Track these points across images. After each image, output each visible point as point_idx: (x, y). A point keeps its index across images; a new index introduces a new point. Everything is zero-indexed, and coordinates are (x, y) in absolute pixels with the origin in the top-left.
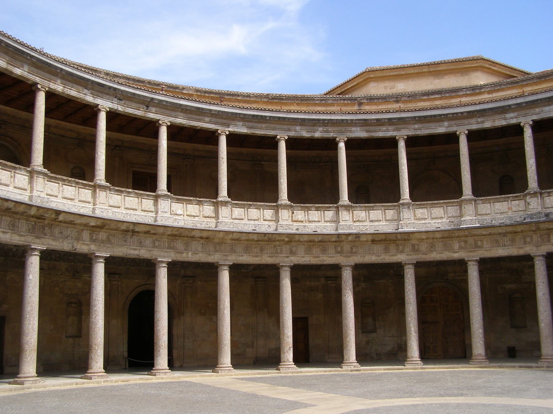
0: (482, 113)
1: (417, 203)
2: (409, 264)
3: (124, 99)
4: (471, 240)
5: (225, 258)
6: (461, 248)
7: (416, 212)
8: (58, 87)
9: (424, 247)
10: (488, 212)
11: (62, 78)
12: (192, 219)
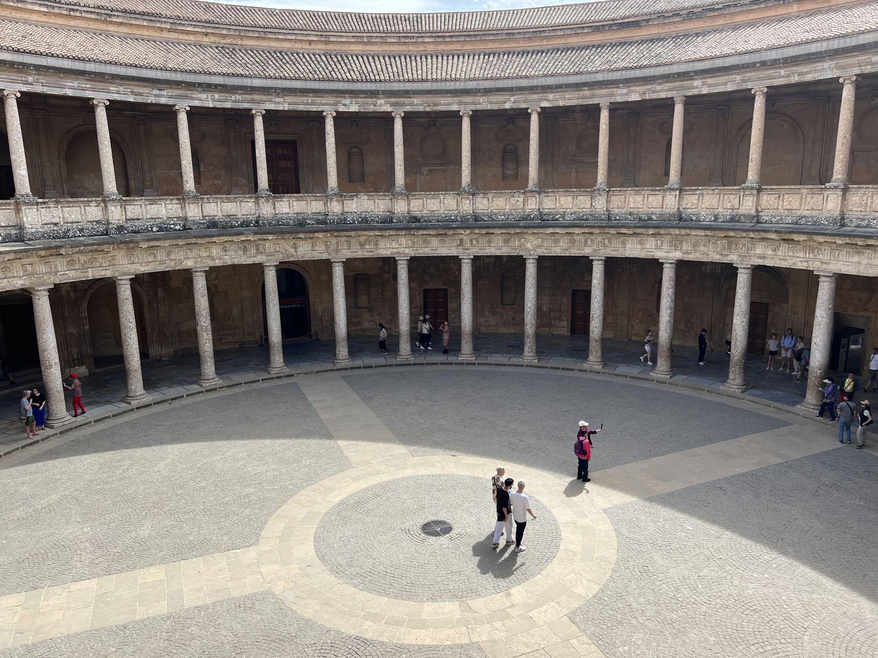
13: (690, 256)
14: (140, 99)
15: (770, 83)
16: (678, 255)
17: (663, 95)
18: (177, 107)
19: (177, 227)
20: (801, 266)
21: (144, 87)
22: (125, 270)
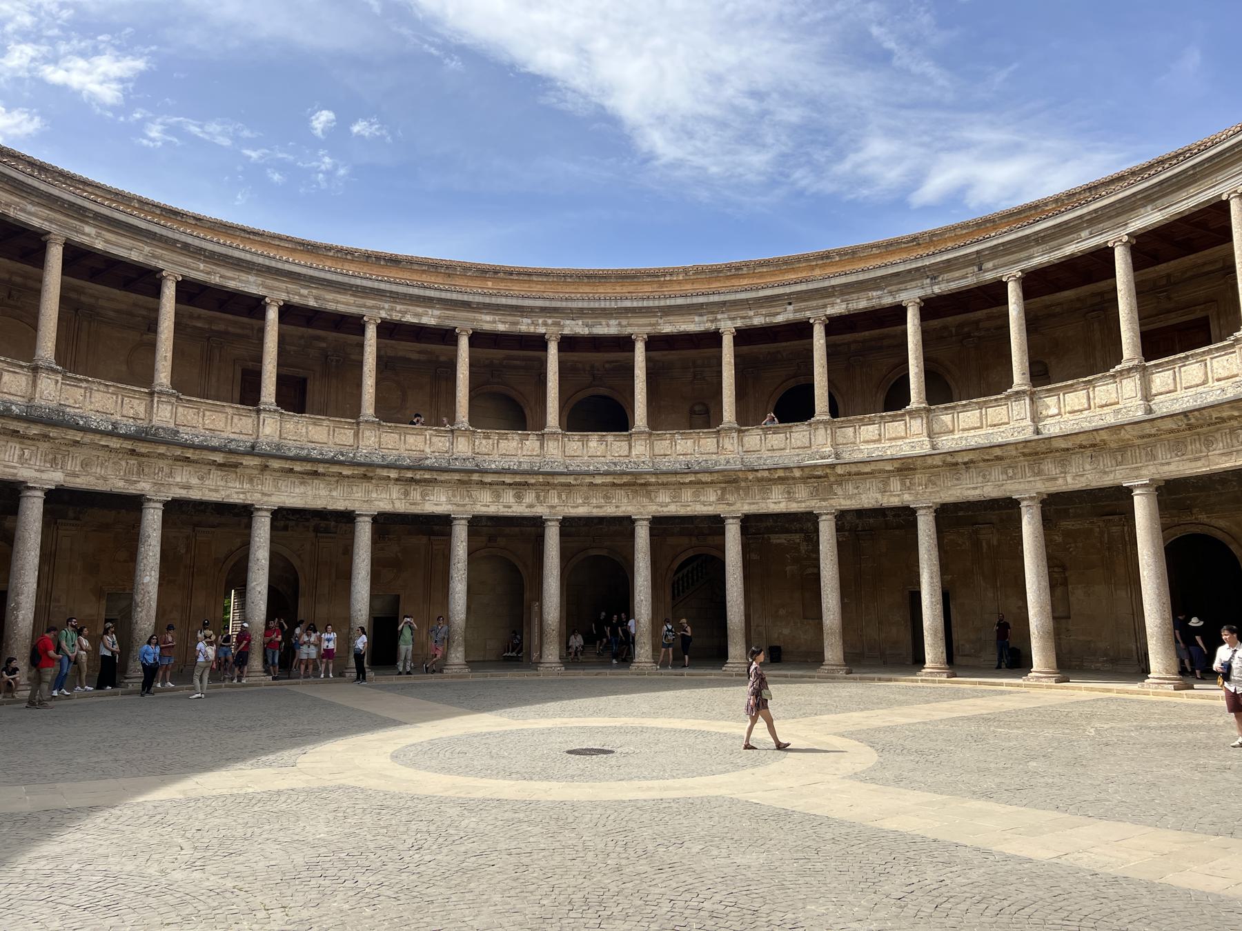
3: (941, 273)
5: (1136, 473)
8: (838, 308)
11: (842, 294)
12: (1078, 416)
13: (78, 480)
15: (185, 272)
16: (55, 477)
17: (36, 222)
20: (236, 498)
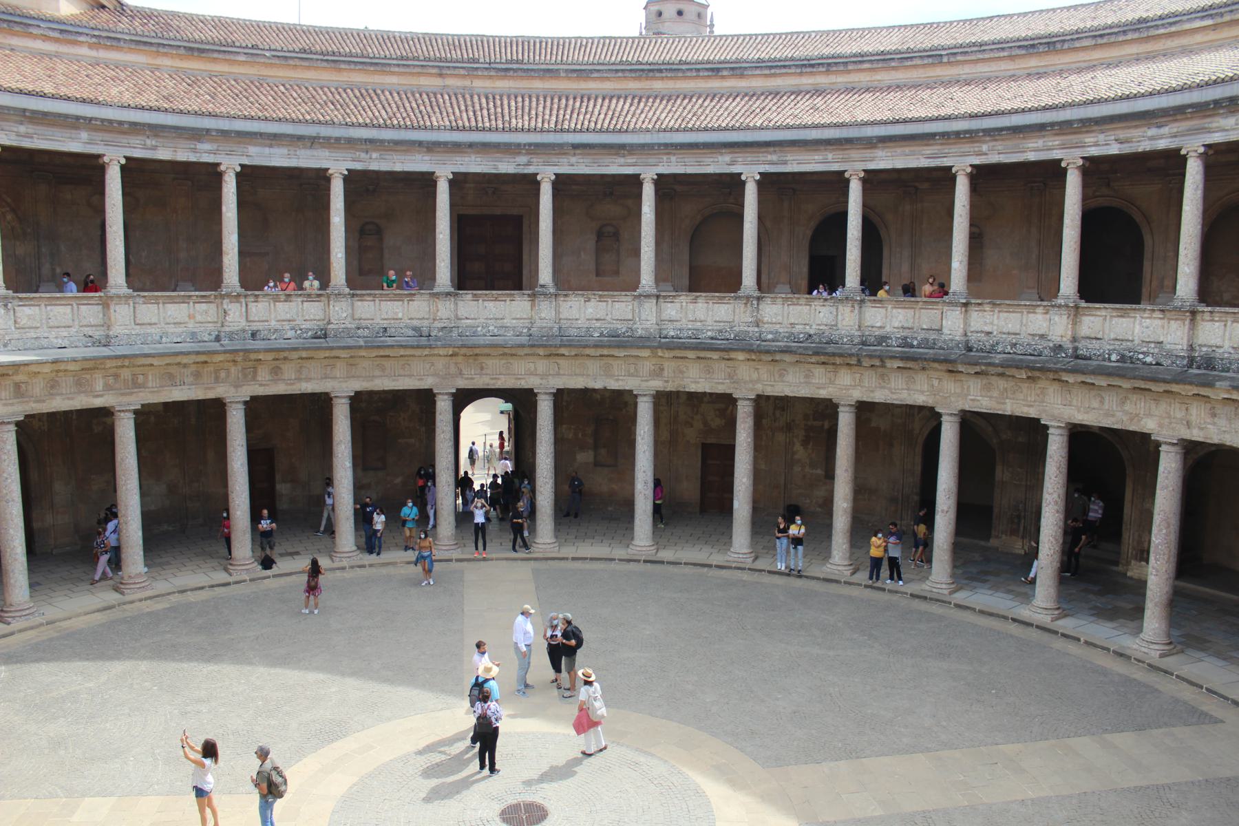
0: (156, 130)
1: (21, 295)
2: (9, 423)
4: (126, 374)
6: (108, 388)
7: (18, 314)
9: (38, 387)
10: (153, 321)
14: (1127, 149)
18: (1183, 152)
19: (1149, 359)
21: (1136, 127)
22: (1056, 412)
